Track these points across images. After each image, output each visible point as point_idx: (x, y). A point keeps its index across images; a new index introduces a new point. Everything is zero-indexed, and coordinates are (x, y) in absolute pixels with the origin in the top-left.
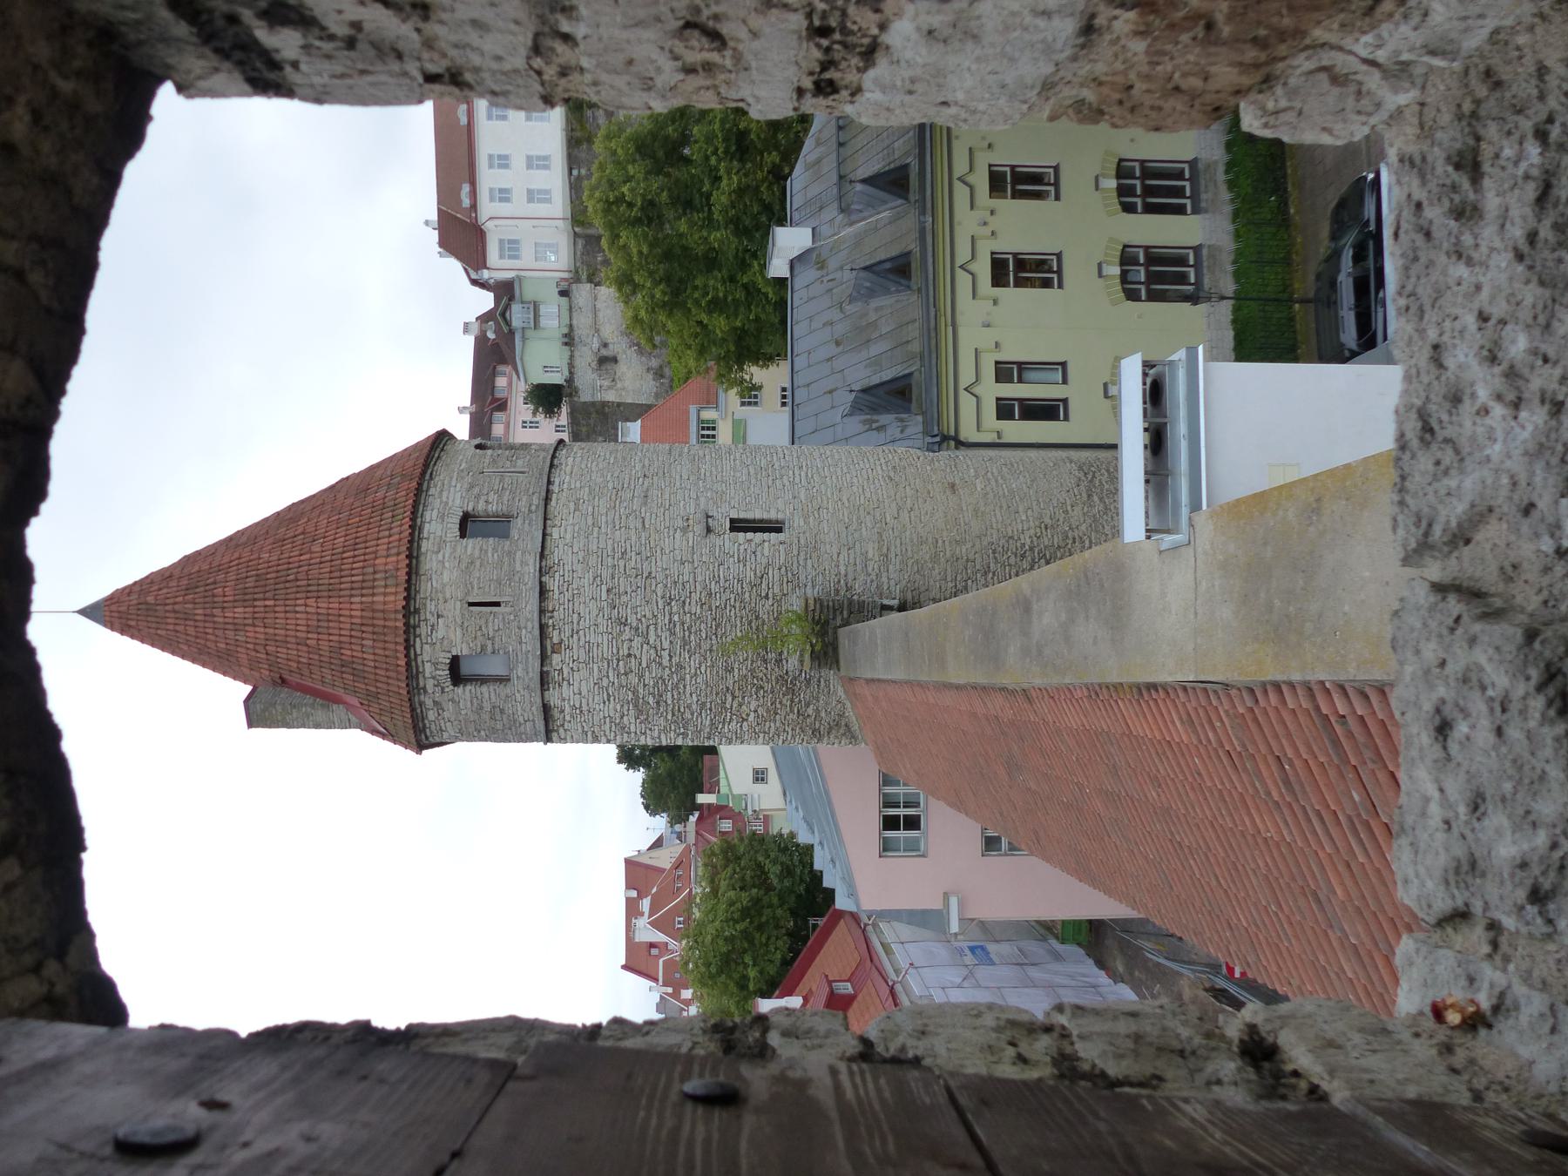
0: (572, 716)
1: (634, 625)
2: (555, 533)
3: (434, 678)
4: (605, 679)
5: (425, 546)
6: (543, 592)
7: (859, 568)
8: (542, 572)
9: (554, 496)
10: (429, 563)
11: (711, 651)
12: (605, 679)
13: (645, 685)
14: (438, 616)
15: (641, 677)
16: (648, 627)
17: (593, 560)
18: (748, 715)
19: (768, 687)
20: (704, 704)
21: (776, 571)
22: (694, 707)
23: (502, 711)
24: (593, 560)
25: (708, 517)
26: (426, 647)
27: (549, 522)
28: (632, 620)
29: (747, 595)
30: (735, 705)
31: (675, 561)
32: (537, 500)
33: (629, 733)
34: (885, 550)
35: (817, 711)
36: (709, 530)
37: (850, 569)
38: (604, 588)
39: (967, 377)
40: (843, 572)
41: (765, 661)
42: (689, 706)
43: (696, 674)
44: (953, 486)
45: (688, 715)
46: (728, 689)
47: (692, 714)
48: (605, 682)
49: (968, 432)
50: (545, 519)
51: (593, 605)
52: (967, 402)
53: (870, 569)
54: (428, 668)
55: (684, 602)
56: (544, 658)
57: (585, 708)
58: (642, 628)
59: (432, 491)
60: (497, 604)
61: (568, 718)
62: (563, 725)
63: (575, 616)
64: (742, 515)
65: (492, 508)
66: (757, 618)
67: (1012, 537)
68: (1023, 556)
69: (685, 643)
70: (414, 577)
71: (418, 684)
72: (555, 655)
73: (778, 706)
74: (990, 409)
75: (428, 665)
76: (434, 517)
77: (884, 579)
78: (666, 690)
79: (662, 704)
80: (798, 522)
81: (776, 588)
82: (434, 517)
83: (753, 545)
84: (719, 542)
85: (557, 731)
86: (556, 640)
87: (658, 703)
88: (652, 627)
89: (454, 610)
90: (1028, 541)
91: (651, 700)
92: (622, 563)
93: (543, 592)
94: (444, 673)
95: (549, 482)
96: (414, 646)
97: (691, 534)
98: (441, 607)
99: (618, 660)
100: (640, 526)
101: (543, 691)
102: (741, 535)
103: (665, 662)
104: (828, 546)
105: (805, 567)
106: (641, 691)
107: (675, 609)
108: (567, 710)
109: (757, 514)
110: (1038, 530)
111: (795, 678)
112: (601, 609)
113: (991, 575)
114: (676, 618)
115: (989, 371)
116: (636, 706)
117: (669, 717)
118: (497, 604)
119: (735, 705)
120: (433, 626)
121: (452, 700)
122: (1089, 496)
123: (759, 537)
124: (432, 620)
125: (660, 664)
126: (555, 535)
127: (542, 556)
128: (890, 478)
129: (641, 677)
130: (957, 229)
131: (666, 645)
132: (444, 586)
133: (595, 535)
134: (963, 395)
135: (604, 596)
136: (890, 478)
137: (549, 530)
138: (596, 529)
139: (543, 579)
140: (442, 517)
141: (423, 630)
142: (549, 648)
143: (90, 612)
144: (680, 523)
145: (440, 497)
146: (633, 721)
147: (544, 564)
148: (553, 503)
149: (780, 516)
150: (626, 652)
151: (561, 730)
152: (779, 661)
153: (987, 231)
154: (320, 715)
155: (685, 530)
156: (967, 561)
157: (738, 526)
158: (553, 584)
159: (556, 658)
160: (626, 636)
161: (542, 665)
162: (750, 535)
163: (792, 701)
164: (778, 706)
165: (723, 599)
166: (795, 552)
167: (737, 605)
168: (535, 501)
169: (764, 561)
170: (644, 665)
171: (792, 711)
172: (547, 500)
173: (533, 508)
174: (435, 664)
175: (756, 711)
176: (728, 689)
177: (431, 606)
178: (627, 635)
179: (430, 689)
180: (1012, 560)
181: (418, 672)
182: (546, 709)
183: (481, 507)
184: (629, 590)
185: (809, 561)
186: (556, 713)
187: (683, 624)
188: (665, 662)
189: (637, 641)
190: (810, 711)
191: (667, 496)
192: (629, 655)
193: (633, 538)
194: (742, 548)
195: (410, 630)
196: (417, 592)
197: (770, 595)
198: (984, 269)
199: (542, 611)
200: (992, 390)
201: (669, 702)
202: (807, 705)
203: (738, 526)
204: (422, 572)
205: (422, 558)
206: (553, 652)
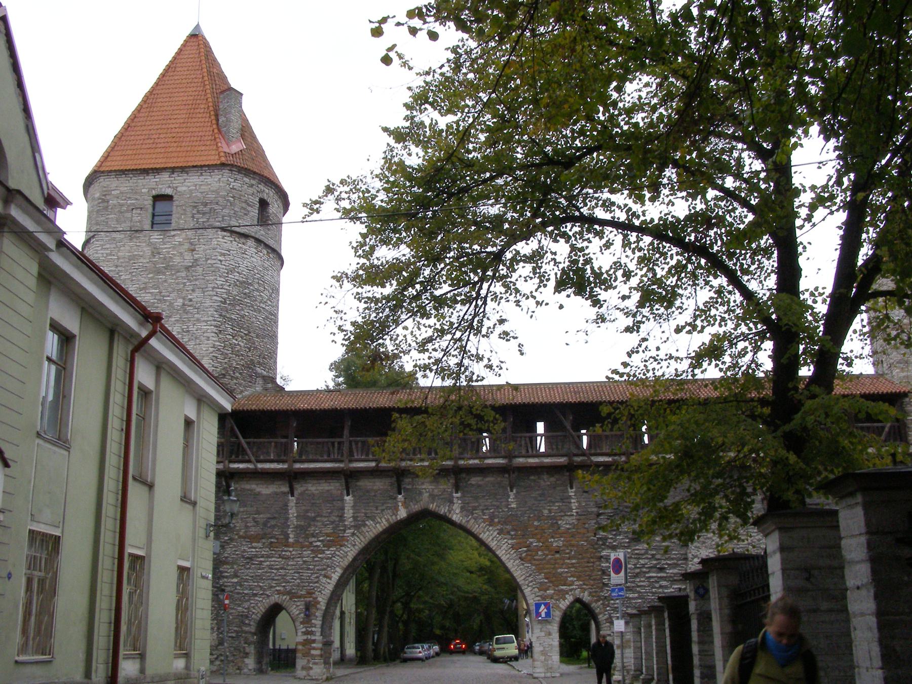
0: (240, 248)
18: (236, 340)
20: (243, 318)
35: (237, 378)
42: (242, 310)
45: (238, 308)
62: (235, 241)
78: (251, 300)
87: (245, 294)
91: (247, 291)
103: (262, 305)
108: (244, 247)
116: (244, 282)
125: (261, 302)
129: (257, 290)
163: (243, 366)
182: (246, 236)
186: (243, 240)
188: (262, 305)
190: (237, 374)
202: (240, 374)
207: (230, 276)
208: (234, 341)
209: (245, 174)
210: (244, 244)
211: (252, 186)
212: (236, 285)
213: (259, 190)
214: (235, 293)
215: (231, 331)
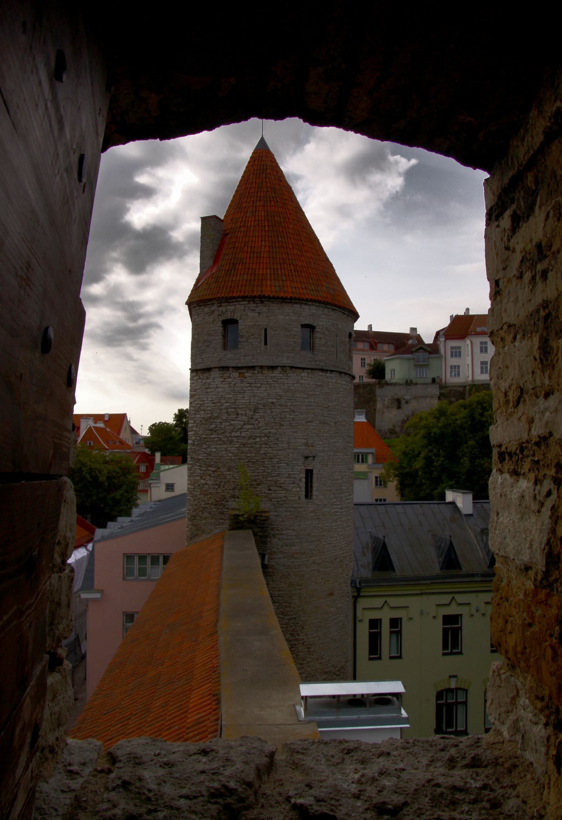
1: (255, 417)
2: (304, 374)
3: (226, 311)
4: (224, 401)
5: (297, 306)
6: (273, 368)
8: (283, 367)
9: (324, 374)
10: (288, 309)
11: (240, 459)
12: (224, 401)
13: (221, 423)
14: (259, 313)
15: (226, 421)
16: (253, 424)
18: (204, 479)
19: (220, 490)
20: (210, 455)
21: (284, 495)
22: (209, 450)
23: (208, 346)
25: (314, 457)
26: (243, 307)
27: (310, 371)
28: (257, 416)
29: (270, 479)
30: (210, 472)
32: (322, 365)
33: (195, 414)
34: (296, 556)
35: (206, 518)
36: (306, 458)
38: (274, 401)
39: (393, 601)
40: (284, 532)
41: (234, 489)
42: (209, 447)
43: (227, 451)
44: (332, 594)
45: (204, 446)
46: (219, 468)
47: (205, 449)
48: (223, 401)
49: (362, 603)
50: (312, 369)
52: (378, 602)
53: (285, 548)
54: (232, 308)
55: (267, 444)
56: (237, 368)
57: (209, 390)
59: (326, 310)
60: (266, 343)
61: (204, 381)
62: (200, 378)
63: (259, 385)
64: (315, 476)
66: (258, 484)
67: (303, 628)
68: (292, 635)
69: (244, 445)
70: (281, 300)
71: (223, 302)
72: (238, 374)
73: (209, 496)
74: (375, 615)
75: (233, 308)
76: (312, 311)
79: (211, 432)
81: (273, 495)
82: (312, 311)
83: (298, 482)
85: (197, 375)
86: (246, 375)
87: (211, 430)
88: (253, 427)
90: (301, 638)
91: (213, 426)
92: (288, 410)
93: (273, 368)
94: (229, 316)
96: (244, 300)
97: (304, 448)
99: (235, 408)
101: (219, 368)
102: (304, 475)
103: (234, 434)
105: (286, 511)
106: (218, 421)
107: (263, 439)
108: (208, 381)
109: (315, 484)
110: (307, 643)
111: (224, 506)
112: (263, 399)
114: (258, 440)
115: (396, 614)
116: (210, 418)
117: (203, 436)
118: (266, 343)
119: (210, 472)
120: (254, 310)
121: (214, 320)
122: (326, 673)
123: (303, 485)
124: (257, 310)
125: (233, 431)
126: (303, 374)
127: (292, 367)
128: (335, 559)
129: (226, 421)
130: (474, 595)
131: (243, 434)
133: (304, 396)
134: (383, 600)
135: (270, 400)
136: (335, 559)
137: (306, 371)
138: (306, 396)
139: (279, 368)
141: (252, 305)
142: (242, 371)
146: (202, 416)
147: (288, 368)
148: (321, 373)
149: (314, 497)
150: (239, 412)
151: (197, 378)
152: (233, 497)
153: (473, 611)
155: (306, 445)
157: (309, 474)
158: (277, 373)
159: (236, 375)
160: (248, 412)
161: (233, 367)
162: (304, 480)
163: (212, 504)
164: (209, 496)
166: (294, 506)
167: (265, 474)
168: (322, 364)
170: (232, 422)
171: (206, 504)
172: (322, 370)
173: (318, 363)
174: (234, 312)
175: (206, 484)
176: (219, 468)
177: (265, 309)
178: (250, 413)
179: (221, 309)
180: (290, 629)
181: (230, 302)
182: (209, 370)
184: (273, 414)
185: (289, 513)
186: (207, 375)
187: (255, 443)
188: (234, 434)
189: (245, 418)
191: (325, 435)
192: (238, 414)
194: (297, 476)
195: (252, 299)
196: (272, 302)
197: (271, 492)
198: (453, 610)
199: (262, 367)
200: (385, 616)
201: (212, 436)
202: (210, 513)
203: (309, 474)
204: (283, 304)
206: (240, 373)
207: (197, 416)
208: (202, 481)
209: (204, 305)
210: (207, 378)
211: (213, 312)
212: (202, 424)
213: (220, 313)
214: (201, 432)
215: (199, 472)
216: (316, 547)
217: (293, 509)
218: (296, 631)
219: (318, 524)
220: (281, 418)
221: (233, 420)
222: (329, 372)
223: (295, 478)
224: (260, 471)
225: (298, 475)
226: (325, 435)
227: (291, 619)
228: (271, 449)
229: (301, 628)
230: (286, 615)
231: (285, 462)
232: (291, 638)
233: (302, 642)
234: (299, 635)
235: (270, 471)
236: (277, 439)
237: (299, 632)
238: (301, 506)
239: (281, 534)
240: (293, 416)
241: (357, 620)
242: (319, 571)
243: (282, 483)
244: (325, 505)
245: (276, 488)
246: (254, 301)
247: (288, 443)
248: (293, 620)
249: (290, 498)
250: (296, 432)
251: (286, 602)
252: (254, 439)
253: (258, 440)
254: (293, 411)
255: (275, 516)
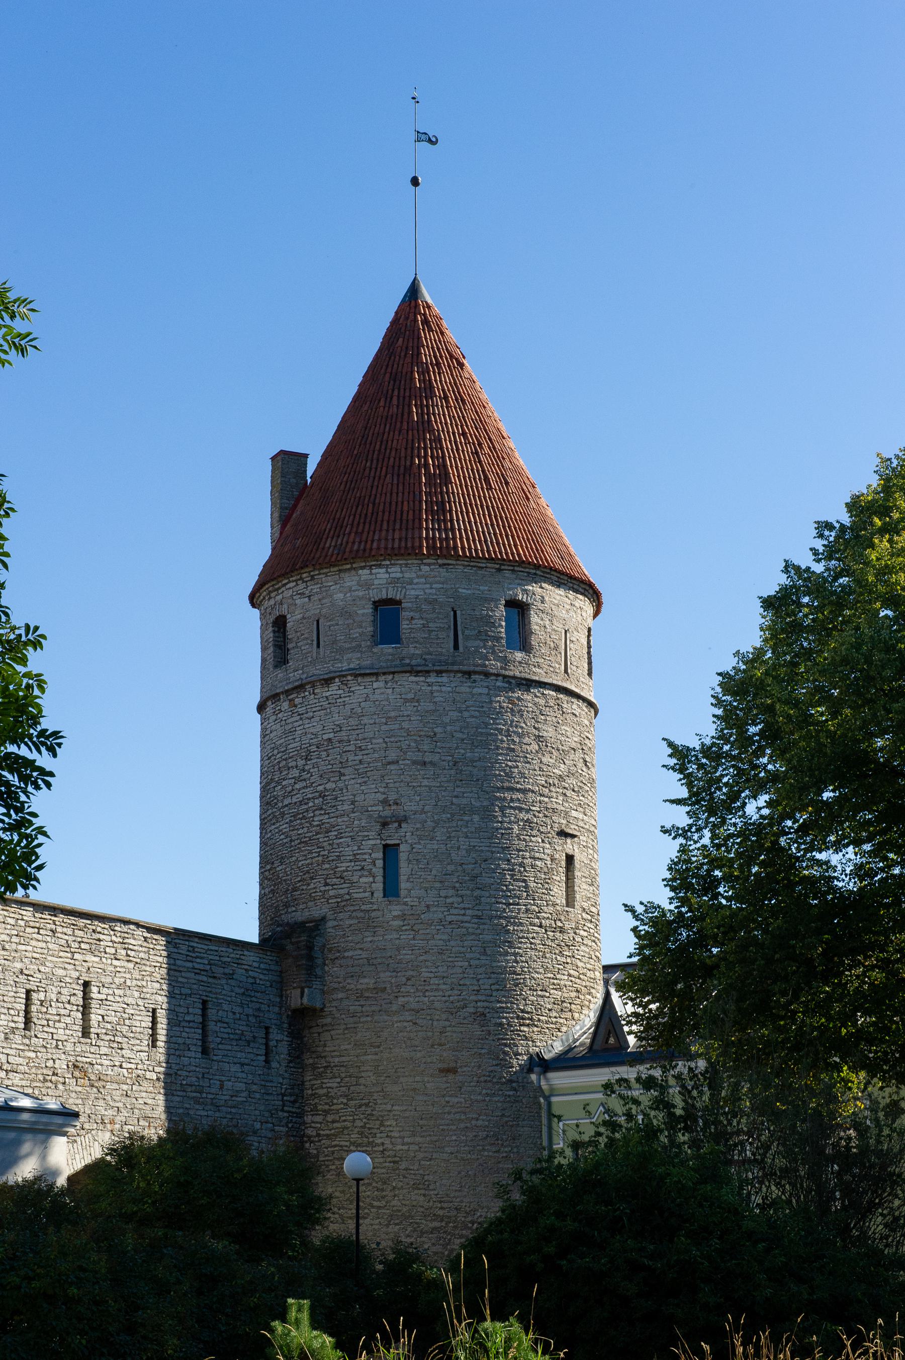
7: (350, 969)
9: (422, 679)
14: (309, 597)
17: (353, 722)
21: (346, 891)
24: (353, 722)
27: (390, 677)
29: (327, 866)
31: (355, 796)
34: (367, 995)
37: (350, 962)
38: (331, 735)
40: (346, 954)
51: (319, 728)
53: (349, 981)
55: (321, 809)
58: (305, 775)
60: (318, 646)
63: (311, 714)
64: (403, 856)
65: (404, 625)
66: (312, 878)
77: (340, 995)
80: (396, 910)
81: (332, 893)
82: (392, 575)
84: (372, 834)
89: (314, 609)
90: (379, 1141)
92: (352, 748)
95: (439, 673)
98: (316, 598)
100: (389, 759)
102: (381, 855)
103: (286, 802)
104: (369, 939)
105: (350, 917)
107: (317, 801)
109: (404, 869)
113: (345, 1101)
118: (318, 646)
120: (303, 594)
123: (378, 871)
126: (375, 685)
131: (294, 800)
132: (331, 596)
135: (326, 737)
137: (382, 678)
138: (384, 720)
139: (337, 680)
140: (394, 582)
143: (414, 291)
144: (392, 797)
145: (418, 577)
147: (349, 678)
148: (412, 678)
149: (403, 893)
154: (276, 515)
155: (385, 802)
156: (358, 1078)
157: (390, 851)
158: (334, 689)
162: (380, 863)
165: (325, 844)
166: (363, 907)
168: (414, 662)
169: (355, 879)
177: (316, 588)
178: (301, 763)
180: (359, 1123)
183: (405, 614)
185: (356, 921)
189: (295, 773)
191: (425, 782)
193: (376, 755)
194: (367, 857)
197: (327, 888)
203: (390, 851)
204: (342, 575)
205: (353, 572)
216: (408, 979)
217: (362, 914)
218: (369, 1129)
219: (414, 939)
220: (341, 763)
221: (284, 779)
222: (433, 675)
223: (365, 860)
224: (314, 855)
225: (370, 855)
226: (425, 782)
227: (360, 1106)
228: (327, 816)
229: (378, 1122)
230: (352, 1099)
231: (347, 834)
232: (360, 1141)
233: (381, 1148)
234: (375, 1136)
235: (326, 853)
236: (336, 798)
237: (374, 1131)
238: (375, 907)
239: (344, 957)
240: (360, 757)
241: (25, 899)
242: (415, 1024)
243: (344, 871)
244: (428, 907)
245: (335, 880)
246: (301, 579)
247: (353, 803)
248: (363, 1108)
249: (355, 896)
250: (365, 782)
251: (350, 1076)
252: (306, 804)
253: (311, 804)
254: (360, 747)
255: (334, 927)
